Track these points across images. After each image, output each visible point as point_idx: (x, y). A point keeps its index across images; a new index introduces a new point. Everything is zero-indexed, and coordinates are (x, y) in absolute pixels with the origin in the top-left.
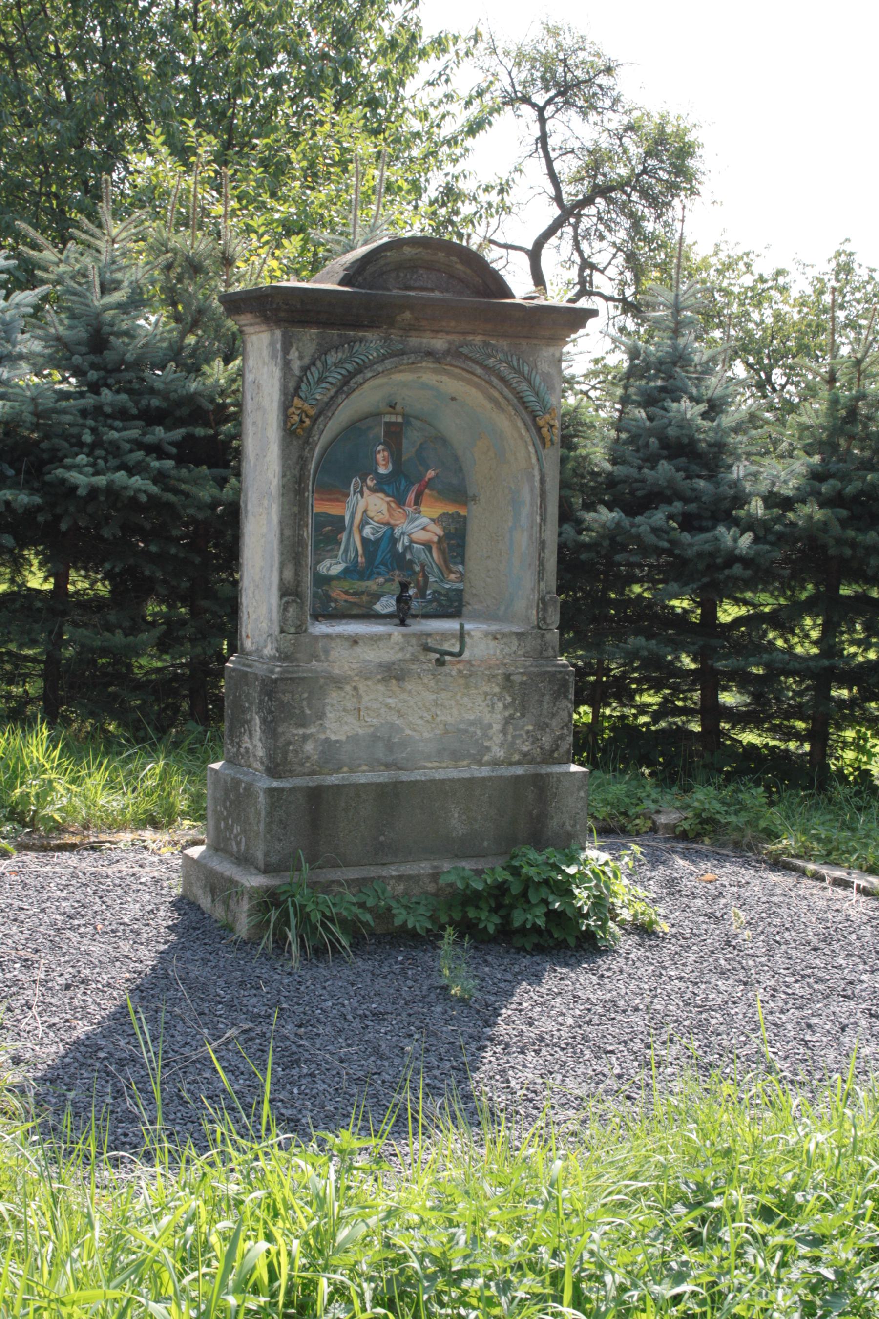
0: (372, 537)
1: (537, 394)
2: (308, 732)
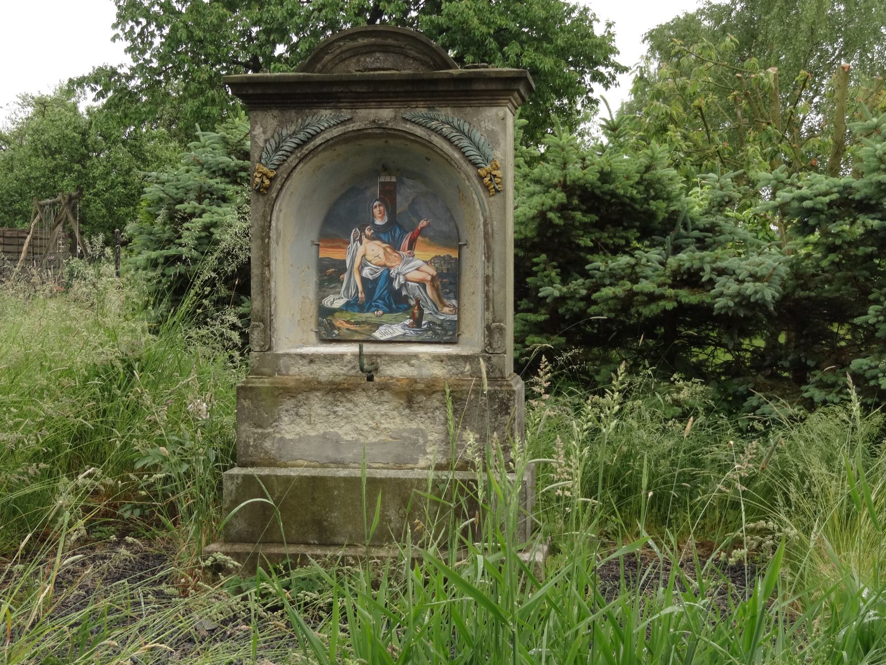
0: (371, 277)
1: (478, 148)
2: (266, 431)
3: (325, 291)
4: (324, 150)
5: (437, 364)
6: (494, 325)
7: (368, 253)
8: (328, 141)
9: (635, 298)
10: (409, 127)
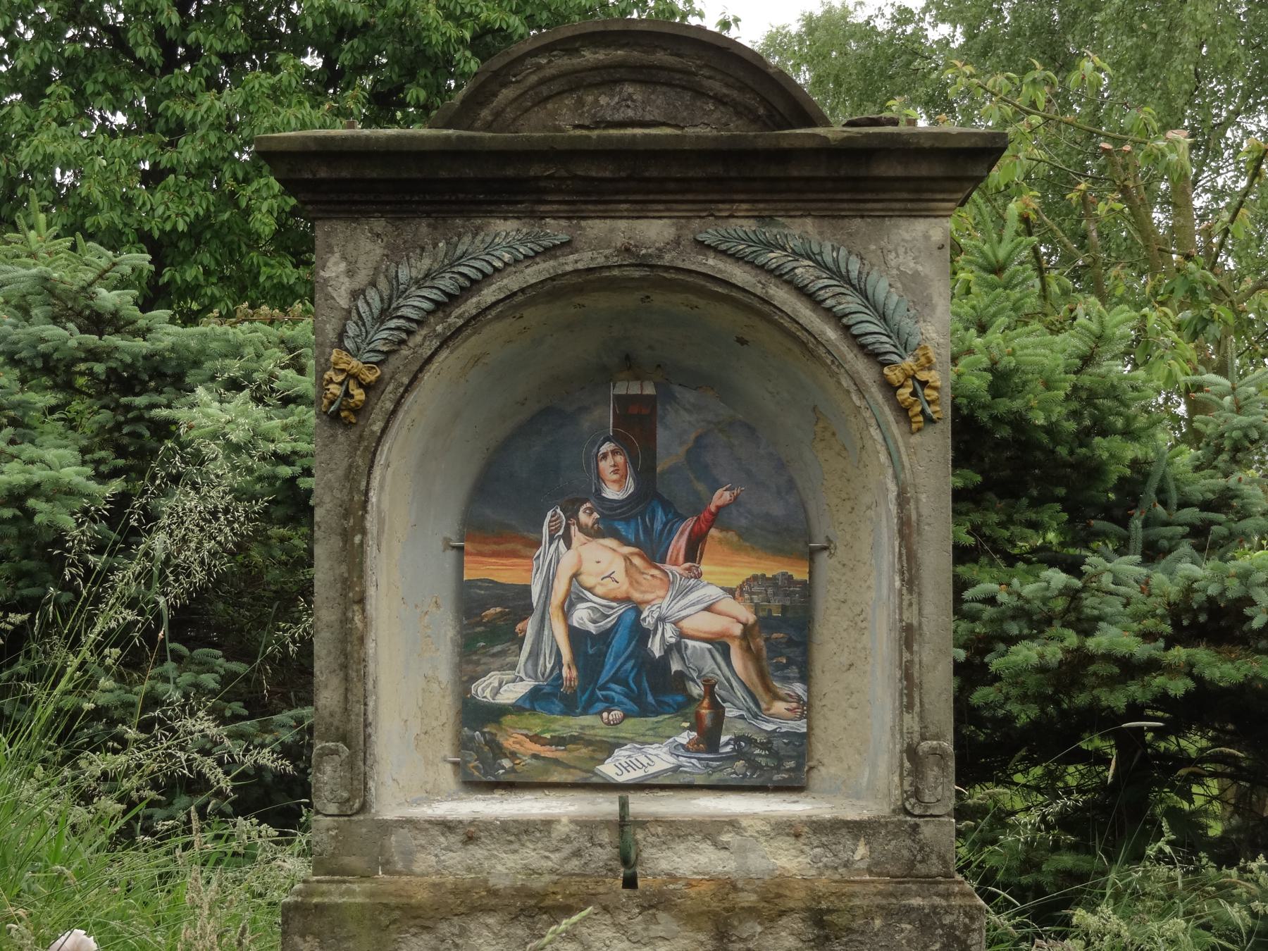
0: (592, 628)
1: (884, 317)
3: (477, 663)
4: (499, 317)
5: (785, 843)
6: (925, 746)
7: (586, 568)
8: (514, 294)
9: (1092, 668)
10: (712, 263)
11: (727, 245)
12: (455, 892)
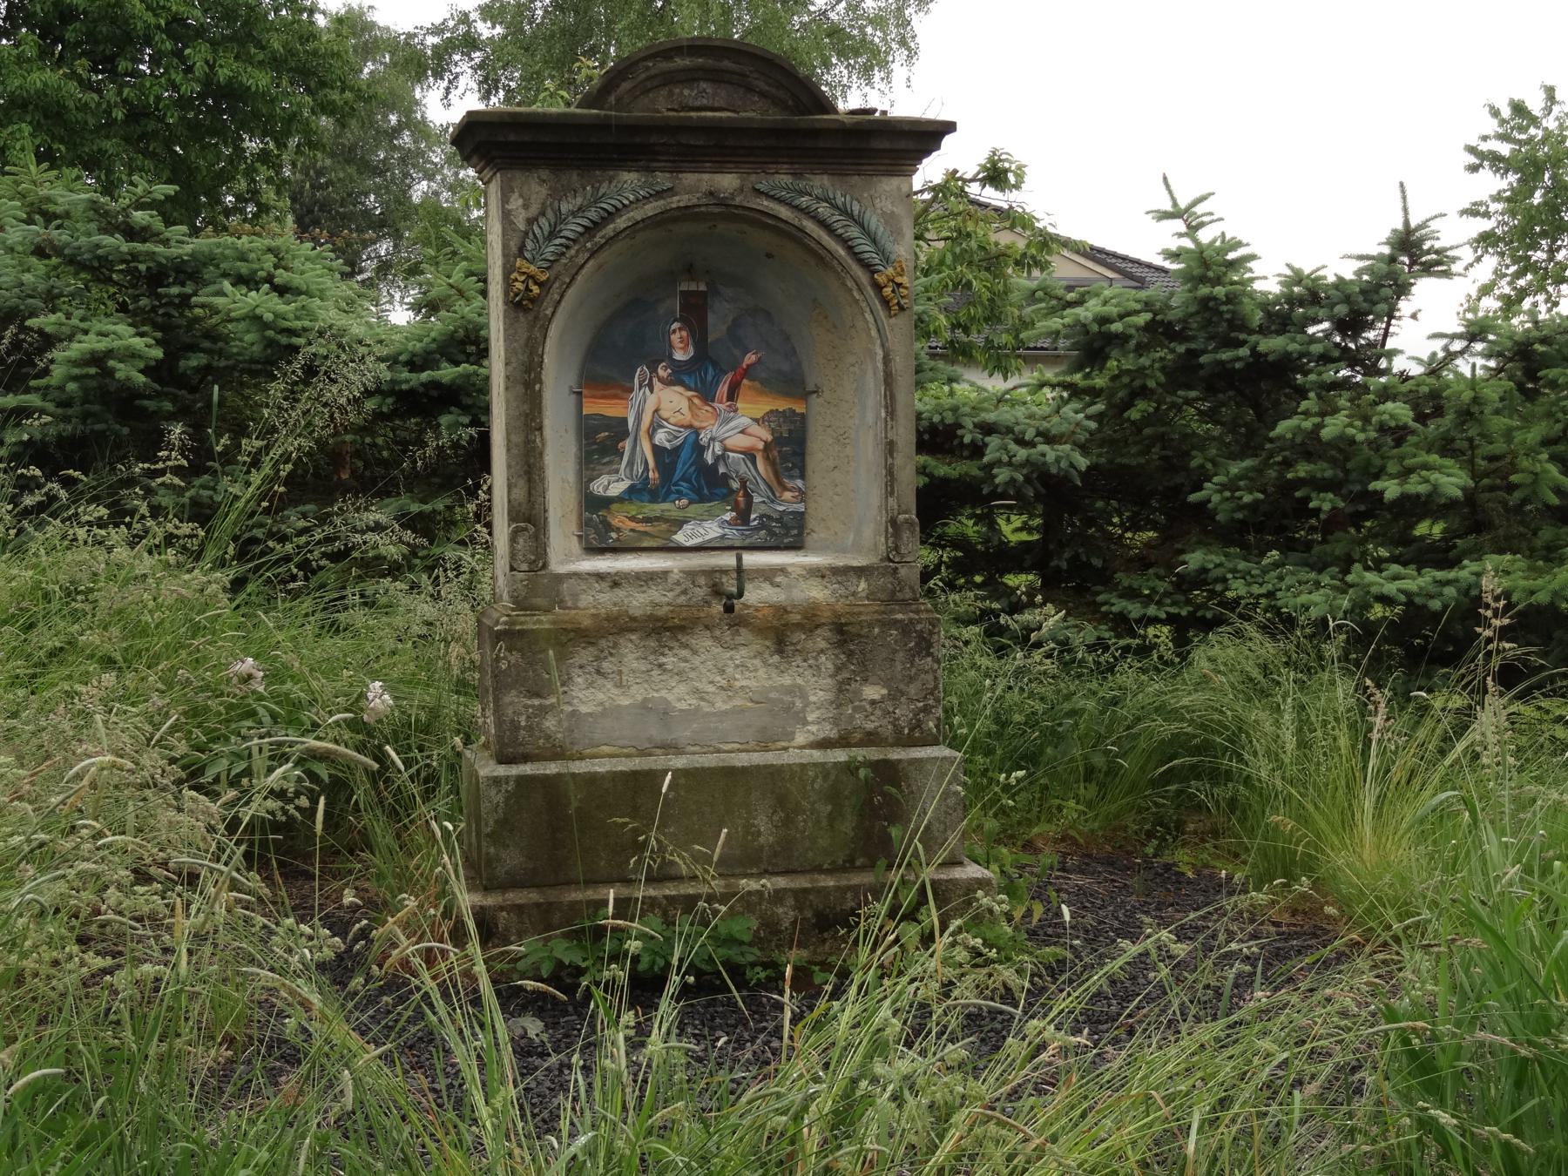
0: (668, 445)
1: (874, 241)
2: (547, 702)
5: (815, 582)
6: (901, 517)
10: (766, 204)
11: (778, 192)
12: (608, 619)
